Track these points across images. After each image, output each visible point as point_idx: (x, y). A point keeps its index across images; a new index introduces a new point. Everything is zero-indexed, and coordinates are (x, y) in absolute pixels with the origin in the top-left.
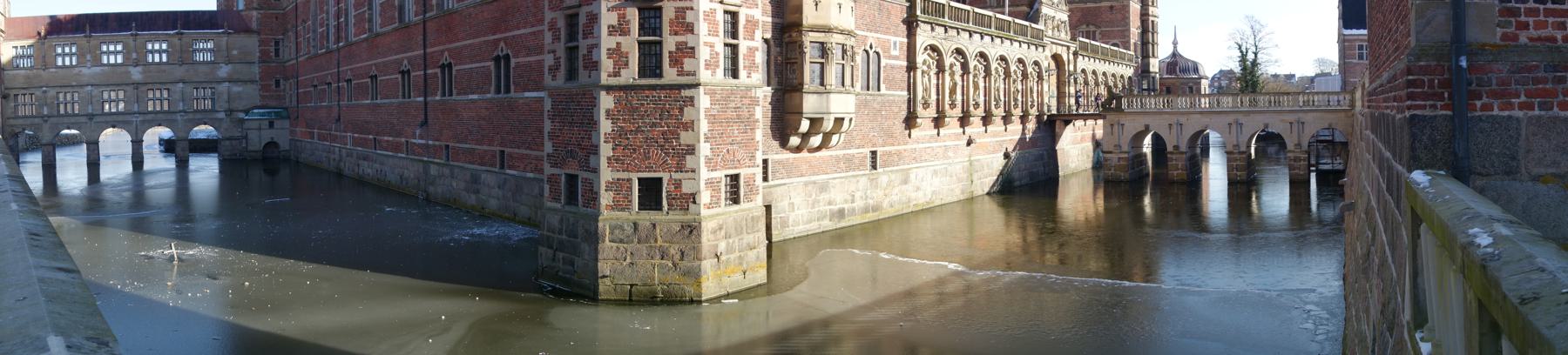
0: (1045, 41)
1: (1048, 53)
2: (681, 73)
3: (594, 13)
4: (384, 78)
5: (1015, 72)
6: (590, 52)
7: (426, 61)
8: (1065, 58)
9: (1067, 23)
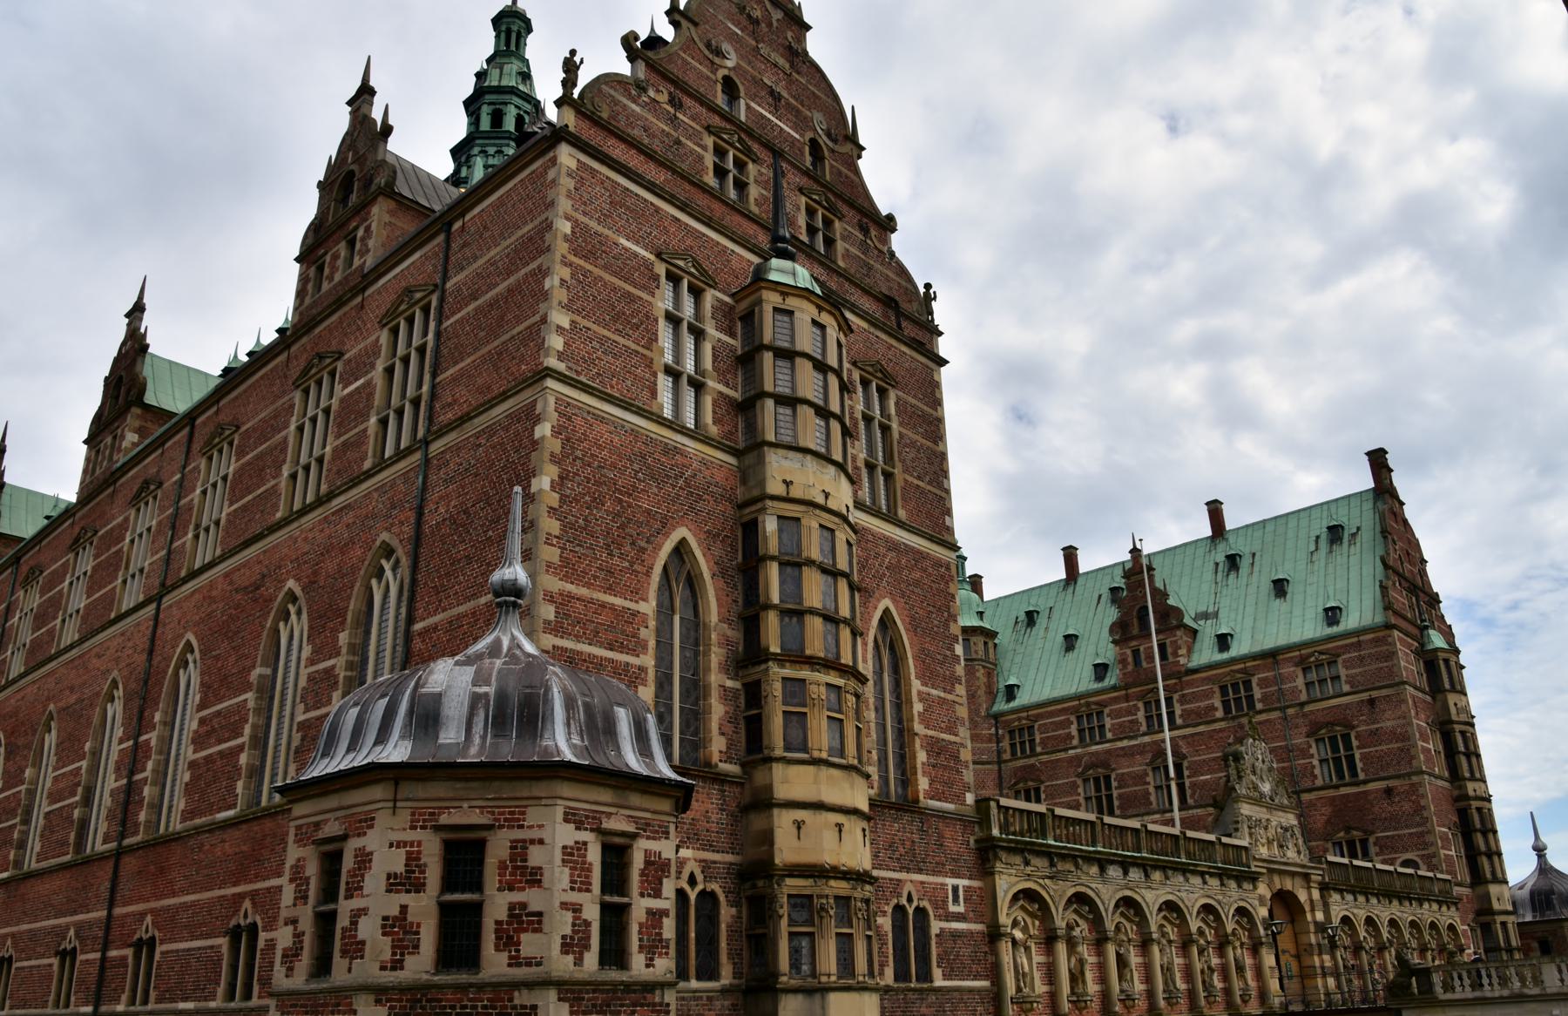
0: (1253, 869)
1: (1263, 889)
2: (515, 962)
3: (368, 849)
4: (26, 964)
5: (1201, 932)
6: (354, 923)
7: (108, 934)
8: (1302, 896)
9: (1297, 831)
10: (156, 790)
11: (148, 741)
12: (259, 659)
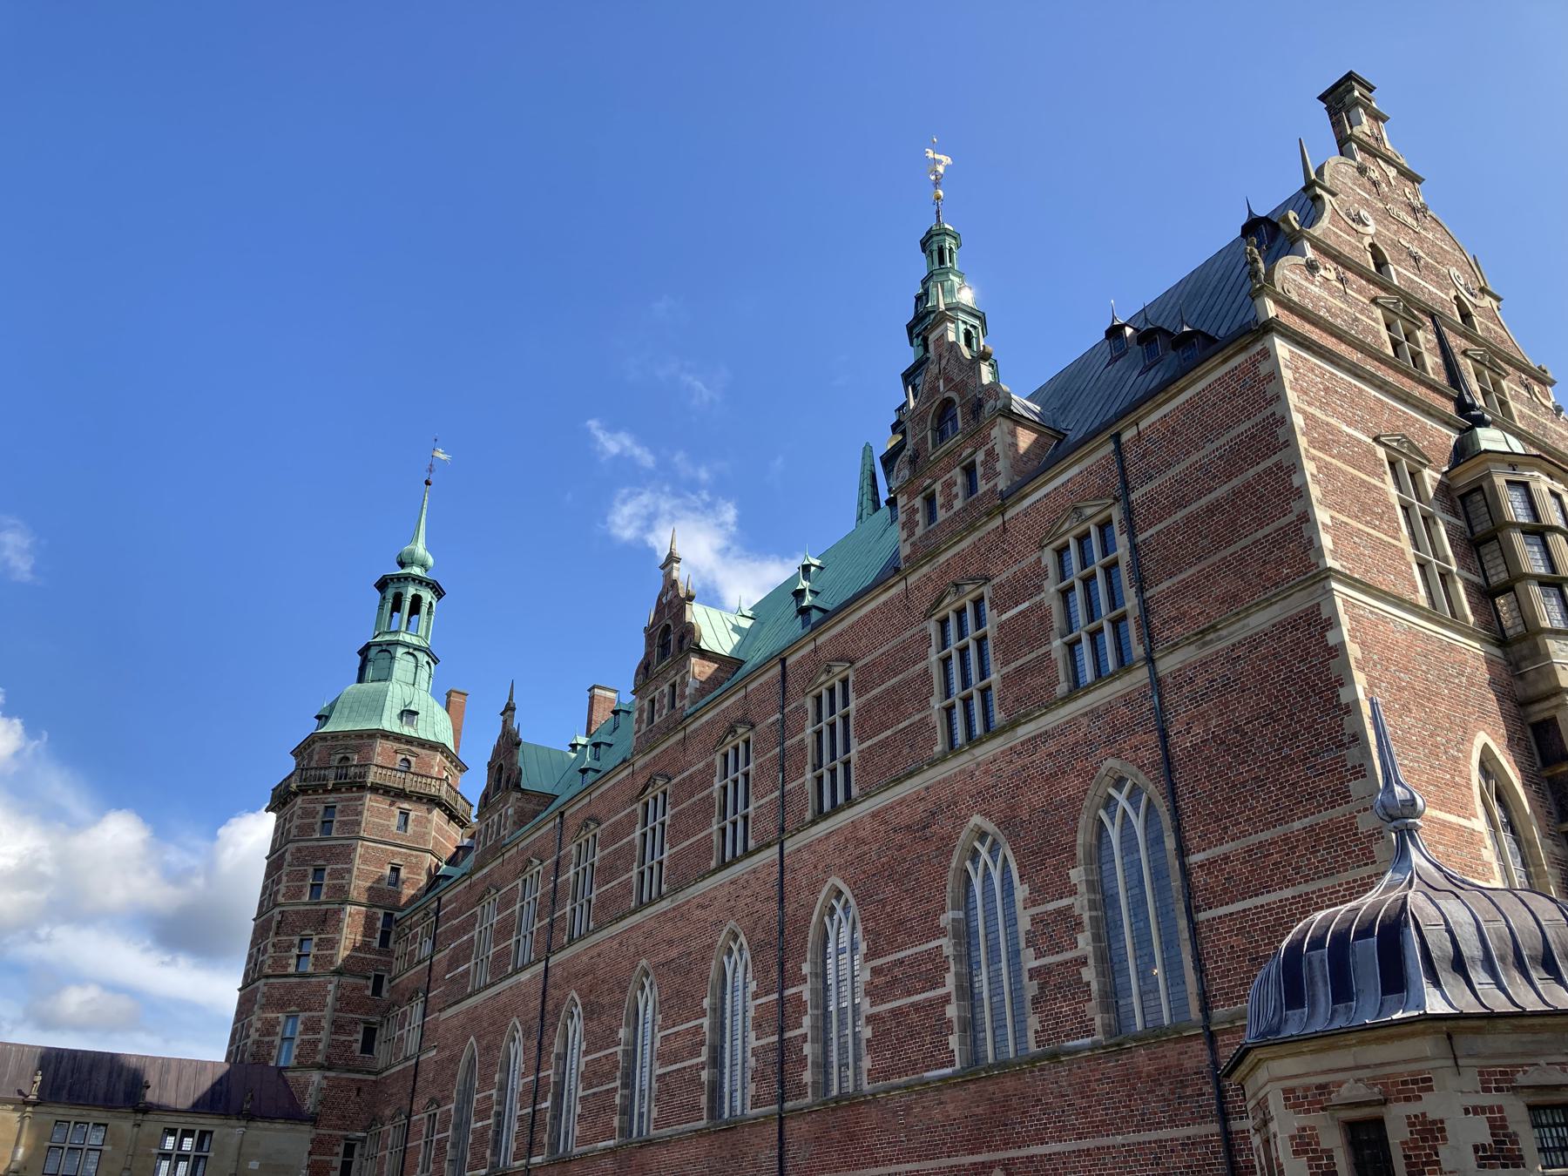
10: (819, 1047)
11: (799, 996)
12: (949, 901)
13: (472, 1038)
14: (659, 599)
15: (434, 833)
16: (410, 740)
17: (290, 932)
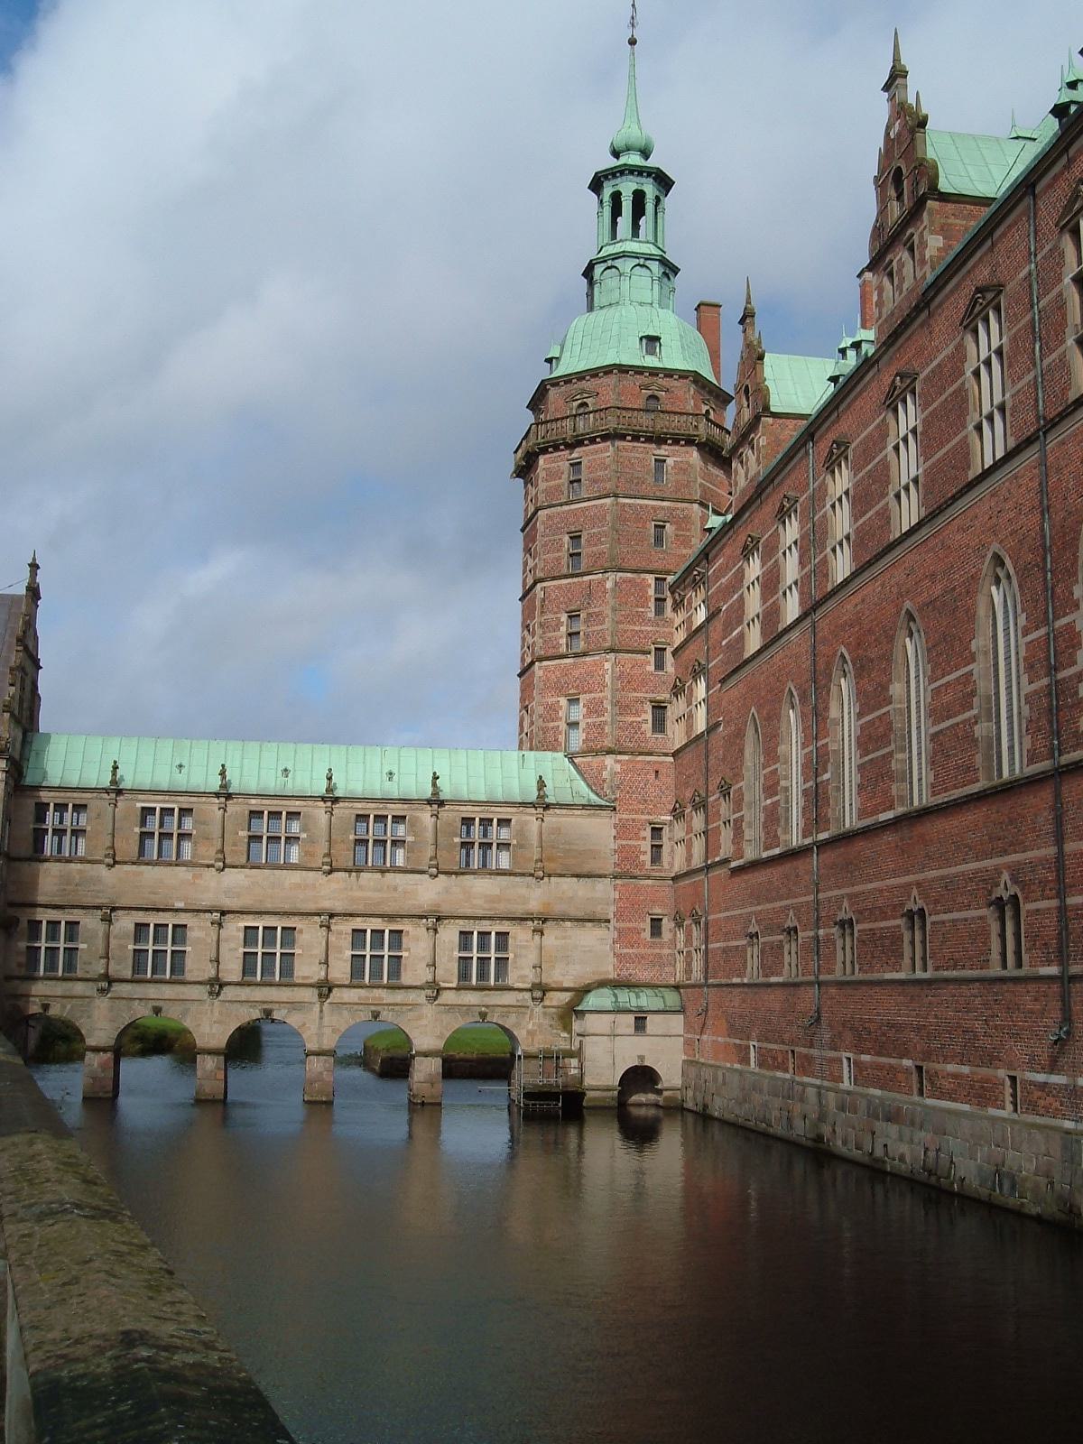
13: (753, 710)
14: (887, 134)
15: (699, 480)
16: (654, 372)
17: (555, 609)
